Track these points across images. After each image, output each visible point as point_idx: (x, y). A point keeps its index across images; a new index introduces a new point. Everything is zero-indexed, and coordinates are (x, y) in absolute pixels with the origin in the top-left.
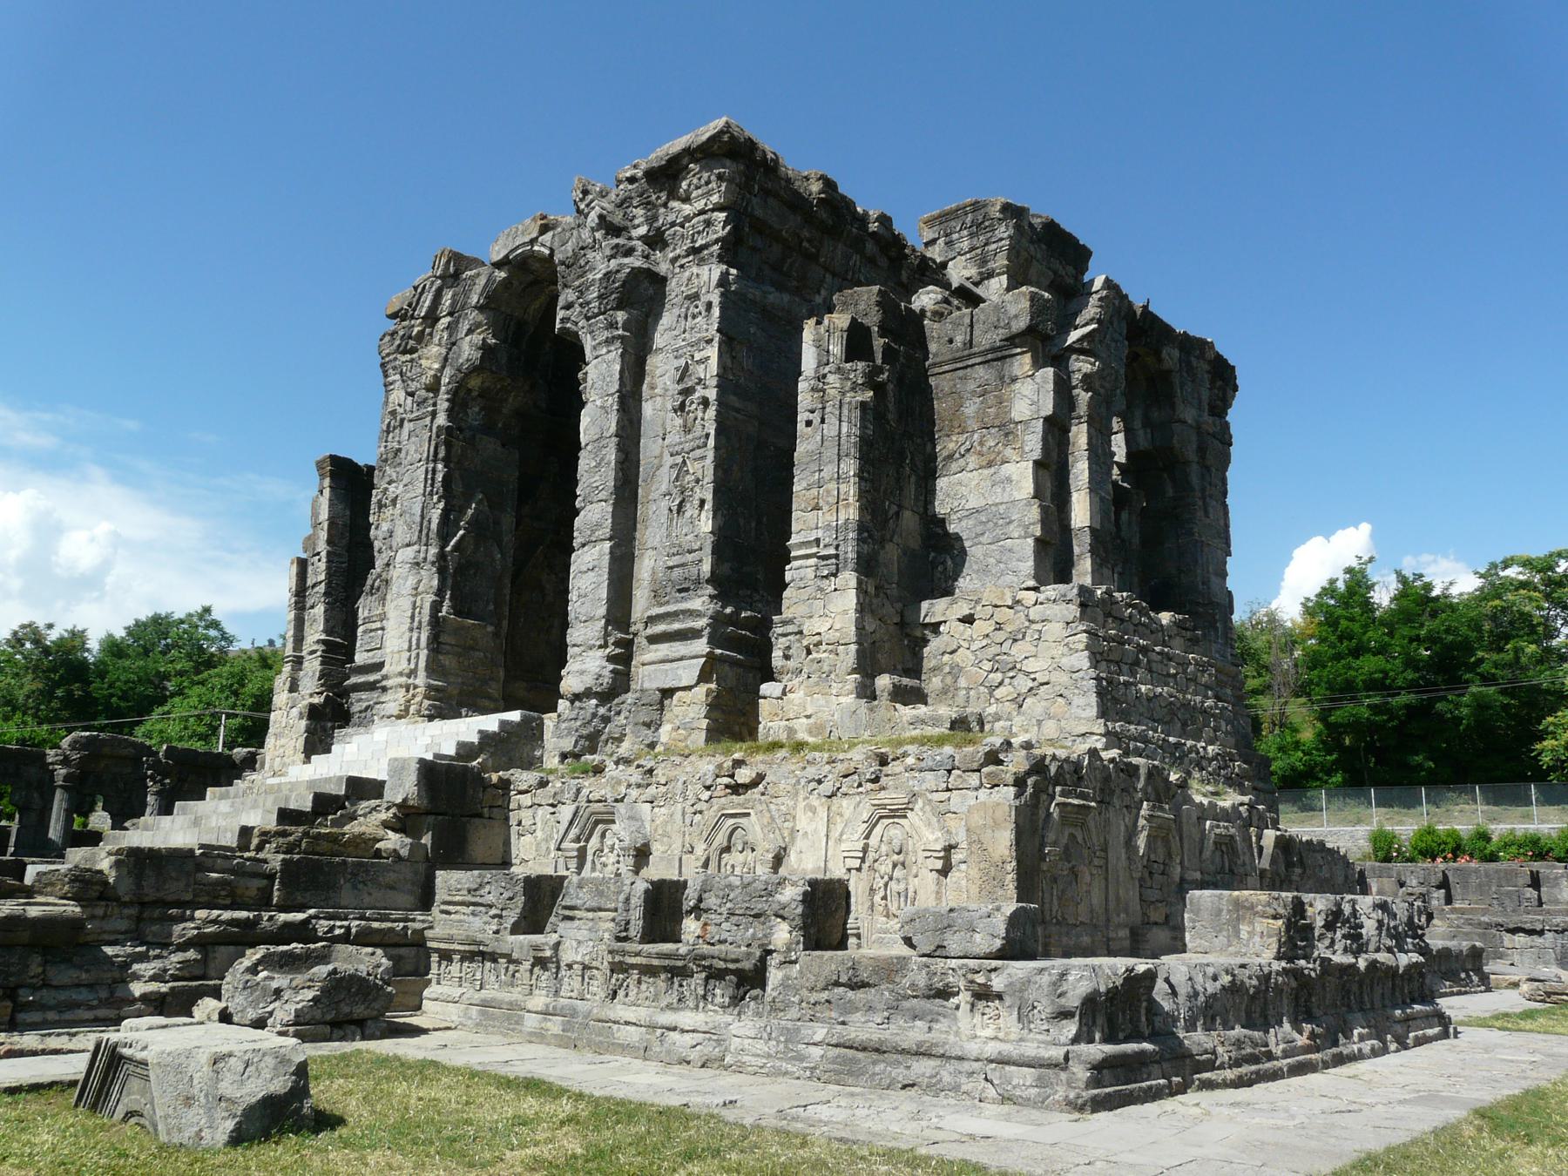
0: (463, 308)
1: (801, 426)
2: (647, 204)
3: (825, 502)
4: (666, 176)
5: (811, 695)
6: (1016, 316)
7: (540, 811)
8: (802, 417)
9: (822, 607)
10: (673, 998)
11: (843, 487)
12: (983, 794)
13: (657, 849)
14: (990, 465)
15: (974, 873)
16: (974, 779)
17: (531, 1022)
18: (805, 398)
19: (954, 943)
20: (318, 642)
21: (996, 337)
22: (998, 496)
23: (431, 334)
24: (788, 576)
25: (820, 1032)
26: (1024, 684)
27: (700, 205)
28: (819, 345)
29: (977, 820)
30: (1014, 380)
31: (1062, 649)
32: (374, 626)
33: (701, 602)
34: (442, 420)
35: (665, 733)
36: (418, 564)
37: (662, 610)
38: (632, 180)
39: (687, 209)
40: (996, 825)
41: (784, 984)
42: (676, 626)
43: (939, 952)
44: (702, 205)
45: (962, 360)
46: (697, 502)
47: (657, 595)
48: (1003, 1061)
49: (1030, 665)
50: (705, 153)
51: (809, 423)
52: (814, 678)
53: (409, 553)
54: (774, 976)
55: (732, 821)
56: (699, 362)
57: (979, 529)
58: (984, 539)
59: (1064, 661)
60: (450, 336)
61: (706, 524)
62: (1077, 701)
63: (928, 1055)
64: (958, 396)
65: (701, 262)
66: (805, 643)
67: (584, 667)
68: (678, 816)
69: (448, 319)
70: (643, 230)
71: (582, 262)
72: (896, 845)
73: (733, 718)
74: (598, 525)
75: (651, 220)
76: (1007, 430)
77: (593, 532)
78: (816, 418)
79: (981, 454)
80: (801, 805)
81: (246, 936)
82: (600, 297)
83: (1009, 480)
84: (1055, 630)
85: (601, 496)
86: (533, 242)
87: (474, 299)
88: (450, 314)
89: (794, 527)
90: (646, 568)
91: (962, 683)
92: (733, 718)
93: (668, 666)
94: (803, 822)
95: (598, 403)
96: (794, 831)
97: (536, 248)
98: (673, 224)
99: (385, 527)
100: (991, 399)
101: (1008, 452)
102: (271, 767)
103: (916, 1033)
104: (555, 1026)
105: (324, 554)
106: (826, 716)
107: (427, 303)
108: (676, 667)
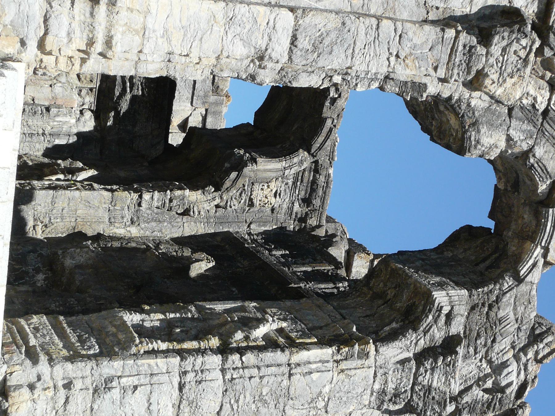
0: (541, 131)
23: (542, 78)
34: (433, 89)
36: (261, 58)
60: (522, 108)
69: (541, 107)
71: (481, 341)
77: (190, 403)
82: (429, 389)
85: (227, 407)
86: (546, 250)
87: (539, 151)
88: (546, 113)
97: (539, 251)
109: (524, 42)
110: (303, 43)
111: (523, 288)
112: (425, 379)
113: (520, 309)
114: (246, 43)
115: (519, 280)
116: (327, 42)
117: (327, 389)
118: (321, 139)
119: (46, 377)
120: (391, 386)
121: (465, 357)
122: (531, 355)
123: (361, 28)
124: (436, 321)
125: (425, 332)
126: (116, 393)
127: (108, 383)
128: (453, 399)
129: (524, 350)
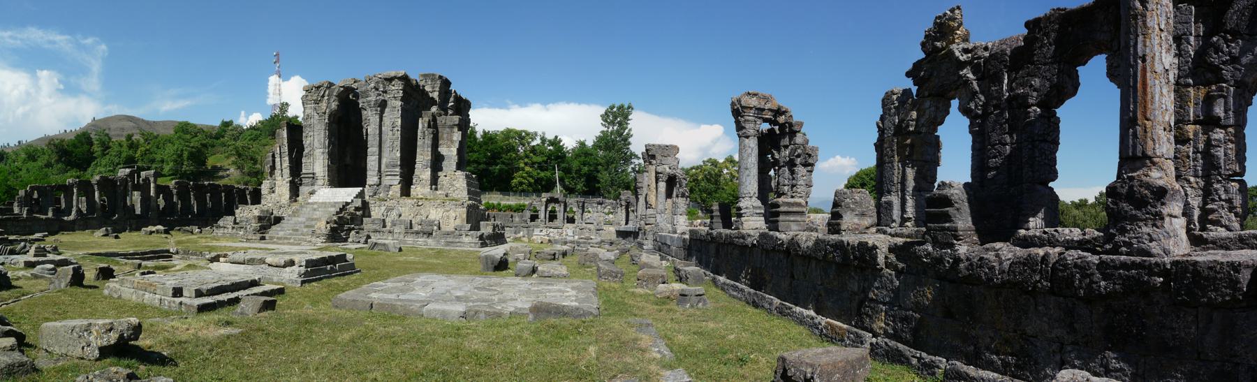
3: (423, 157)
4: (390, 80)
5: (420, 188)
9: (423, 173)
18: (419, 134)
28: (422, 124)
33: (398, 169)
44: (397, 88)
45: (444, 125)
50: (400, 79)
61: (398, 155)
64: (444, 133)
67: (372, 179)
73: (406, 192)
76: (452, 142)
81: (350, 230)
90: (384, 161)
92: (406, 192)
108: (394, 182)
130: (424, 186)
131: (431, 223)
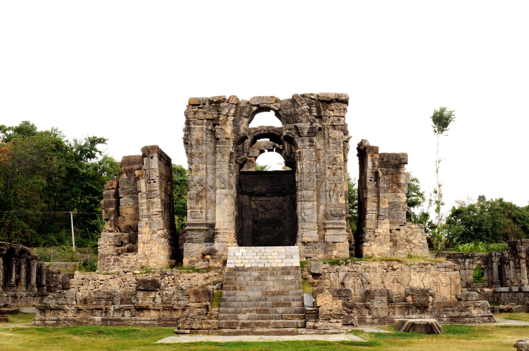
1: (368, 181)
2: (318, 108)
6: (403, 159)
7: (331, 274)
8: (368, 179)
10: (406, 313)
11: (385, 199)
12: (453, 272)
13: (373, 283)
14: (394, 192)
15: (453, 286)
16: (451, 270)
17: (368, 321)
19: (469, 299)
20: (159, 212)
21: (397, 162)
22: (397, 200)
24: (367, 217)
25: (445, 316)
26: (413, 246)
27: (337, 114)
29: (452, 277)
30: (400, 173)
31: (420, 239)
32: (196, 210)
35: (335, 253)
37: (328, 221)
38: (314, 99)
39: (332, 113)
40: (457, 278)
41: (434, 308)
42: (335, 226)
43: (467, 300)
46: (339, 195)
47: (326, 216)
48: (482, 316)
49: (414, 241)
51: (371, 180)
52: (379, 243)
53: (224, 191)
54: (430, 307)
55: (393, 277)
56: (337, 157)
57: (392, 207)
58: (393, 210)
59: (422, 241)
62: (425, 250)
63: (468, 317)
65: (335, 129)
66: (376, 234)
68: (378, 276)
70: (315, 114)
72: (435, 281)
74: (312, 197)
75: (319, 112)
76: (399, 185)
78: (373, 179)
79: (392, 189)
80: (412, 274)
83: (399, 197)
84: (420, 234)
87: (244, 114)
89: (368, 206)
91: (398, 243)
93: (335, 236)
94: (413, 277)
95: (308, 162)
96: (410, 279)
98: (327, 116)
99: (197, 178)
100: (394, 176)
101: (399, 190)
102: (144, 253)
103: (464, 314)
104: (376, 321)
105: (157, 180)
106: (382, 251)
107: (227, 111)
109: (217, 130)
110: (223, 186)
111: (282, 108)
112: (306, 134)
113: (288, 107)
114: (224, 200)
115: (280, 110)
116: (222, 180)
117: (308, 162)
118: (277, 133)
119: (301, 233)
120: (308, 144)
121: (301, 122)
122: (299, 103)
123: (218, 173)
124: (290, 133)
125: (294, 136)
126: (305, 217)
127: (304, 220)
128: (312, 124)
129: (298, 104)
130: (381, 244)
131: (425, 293)
